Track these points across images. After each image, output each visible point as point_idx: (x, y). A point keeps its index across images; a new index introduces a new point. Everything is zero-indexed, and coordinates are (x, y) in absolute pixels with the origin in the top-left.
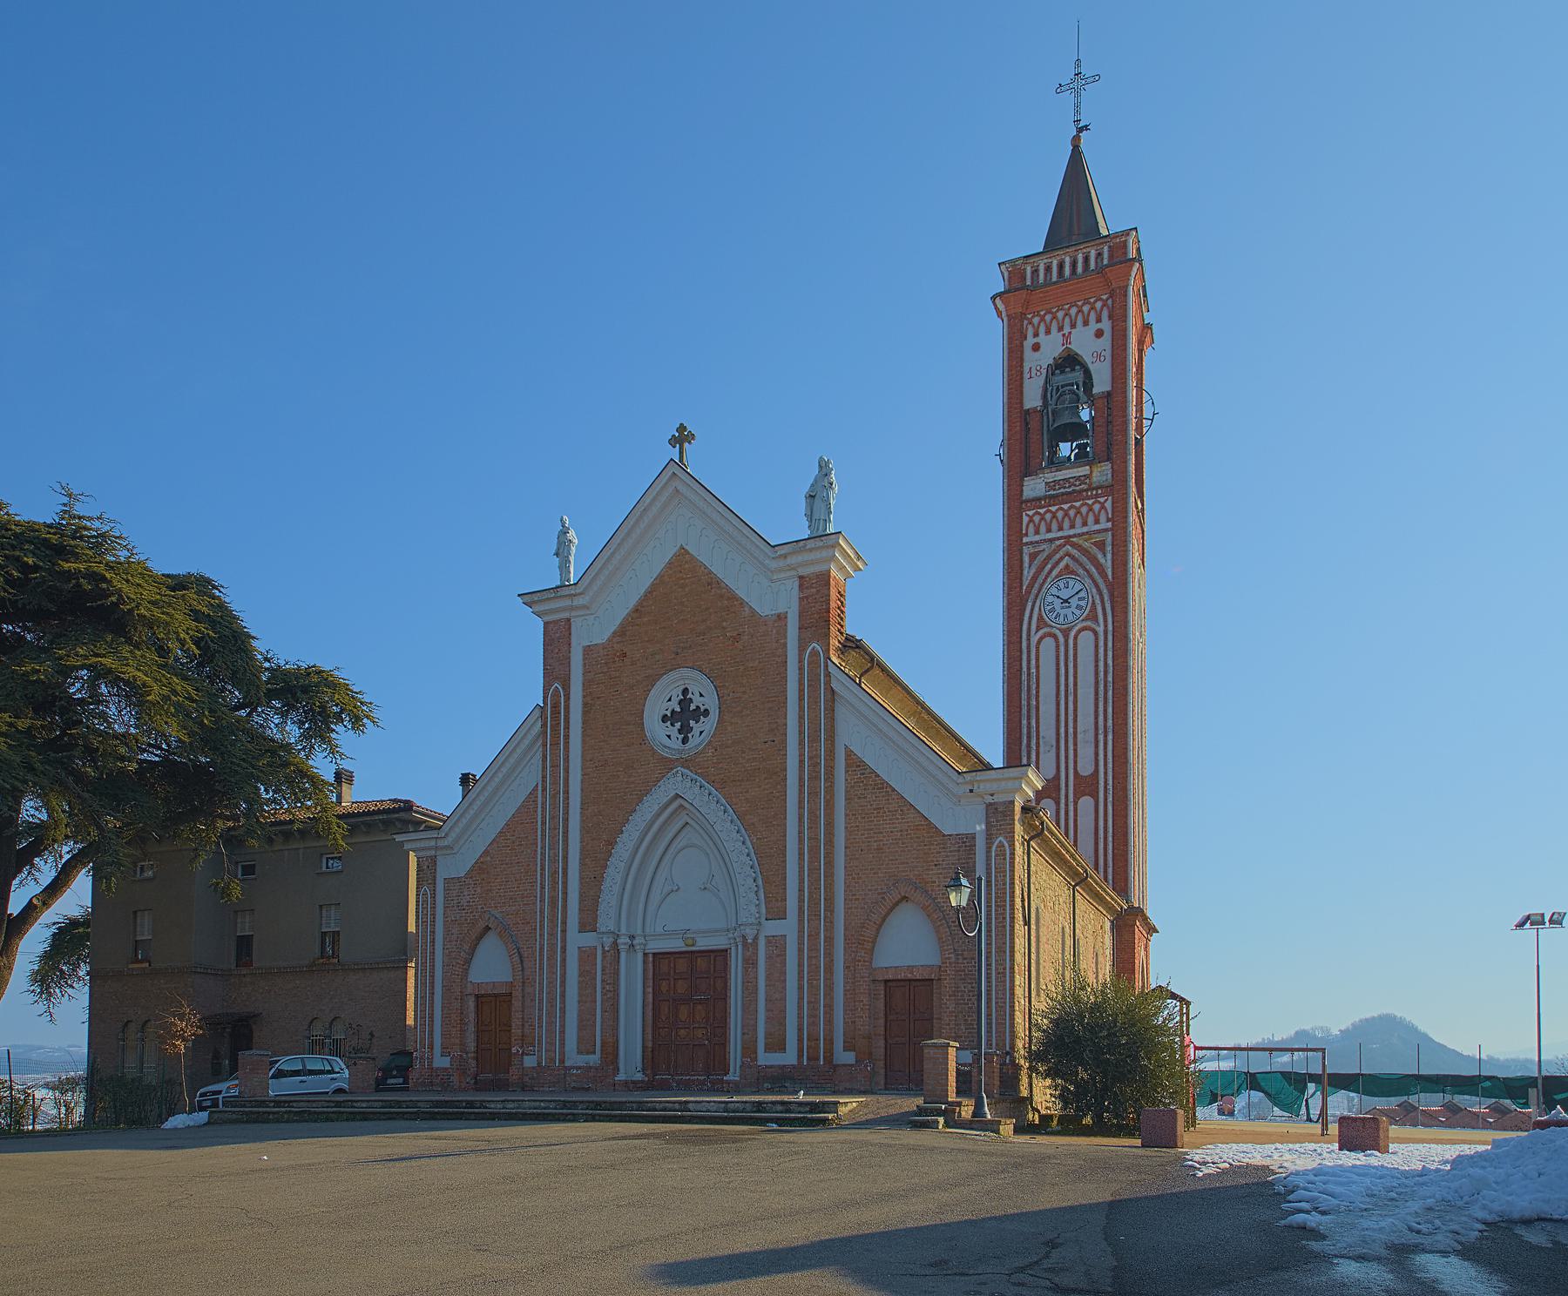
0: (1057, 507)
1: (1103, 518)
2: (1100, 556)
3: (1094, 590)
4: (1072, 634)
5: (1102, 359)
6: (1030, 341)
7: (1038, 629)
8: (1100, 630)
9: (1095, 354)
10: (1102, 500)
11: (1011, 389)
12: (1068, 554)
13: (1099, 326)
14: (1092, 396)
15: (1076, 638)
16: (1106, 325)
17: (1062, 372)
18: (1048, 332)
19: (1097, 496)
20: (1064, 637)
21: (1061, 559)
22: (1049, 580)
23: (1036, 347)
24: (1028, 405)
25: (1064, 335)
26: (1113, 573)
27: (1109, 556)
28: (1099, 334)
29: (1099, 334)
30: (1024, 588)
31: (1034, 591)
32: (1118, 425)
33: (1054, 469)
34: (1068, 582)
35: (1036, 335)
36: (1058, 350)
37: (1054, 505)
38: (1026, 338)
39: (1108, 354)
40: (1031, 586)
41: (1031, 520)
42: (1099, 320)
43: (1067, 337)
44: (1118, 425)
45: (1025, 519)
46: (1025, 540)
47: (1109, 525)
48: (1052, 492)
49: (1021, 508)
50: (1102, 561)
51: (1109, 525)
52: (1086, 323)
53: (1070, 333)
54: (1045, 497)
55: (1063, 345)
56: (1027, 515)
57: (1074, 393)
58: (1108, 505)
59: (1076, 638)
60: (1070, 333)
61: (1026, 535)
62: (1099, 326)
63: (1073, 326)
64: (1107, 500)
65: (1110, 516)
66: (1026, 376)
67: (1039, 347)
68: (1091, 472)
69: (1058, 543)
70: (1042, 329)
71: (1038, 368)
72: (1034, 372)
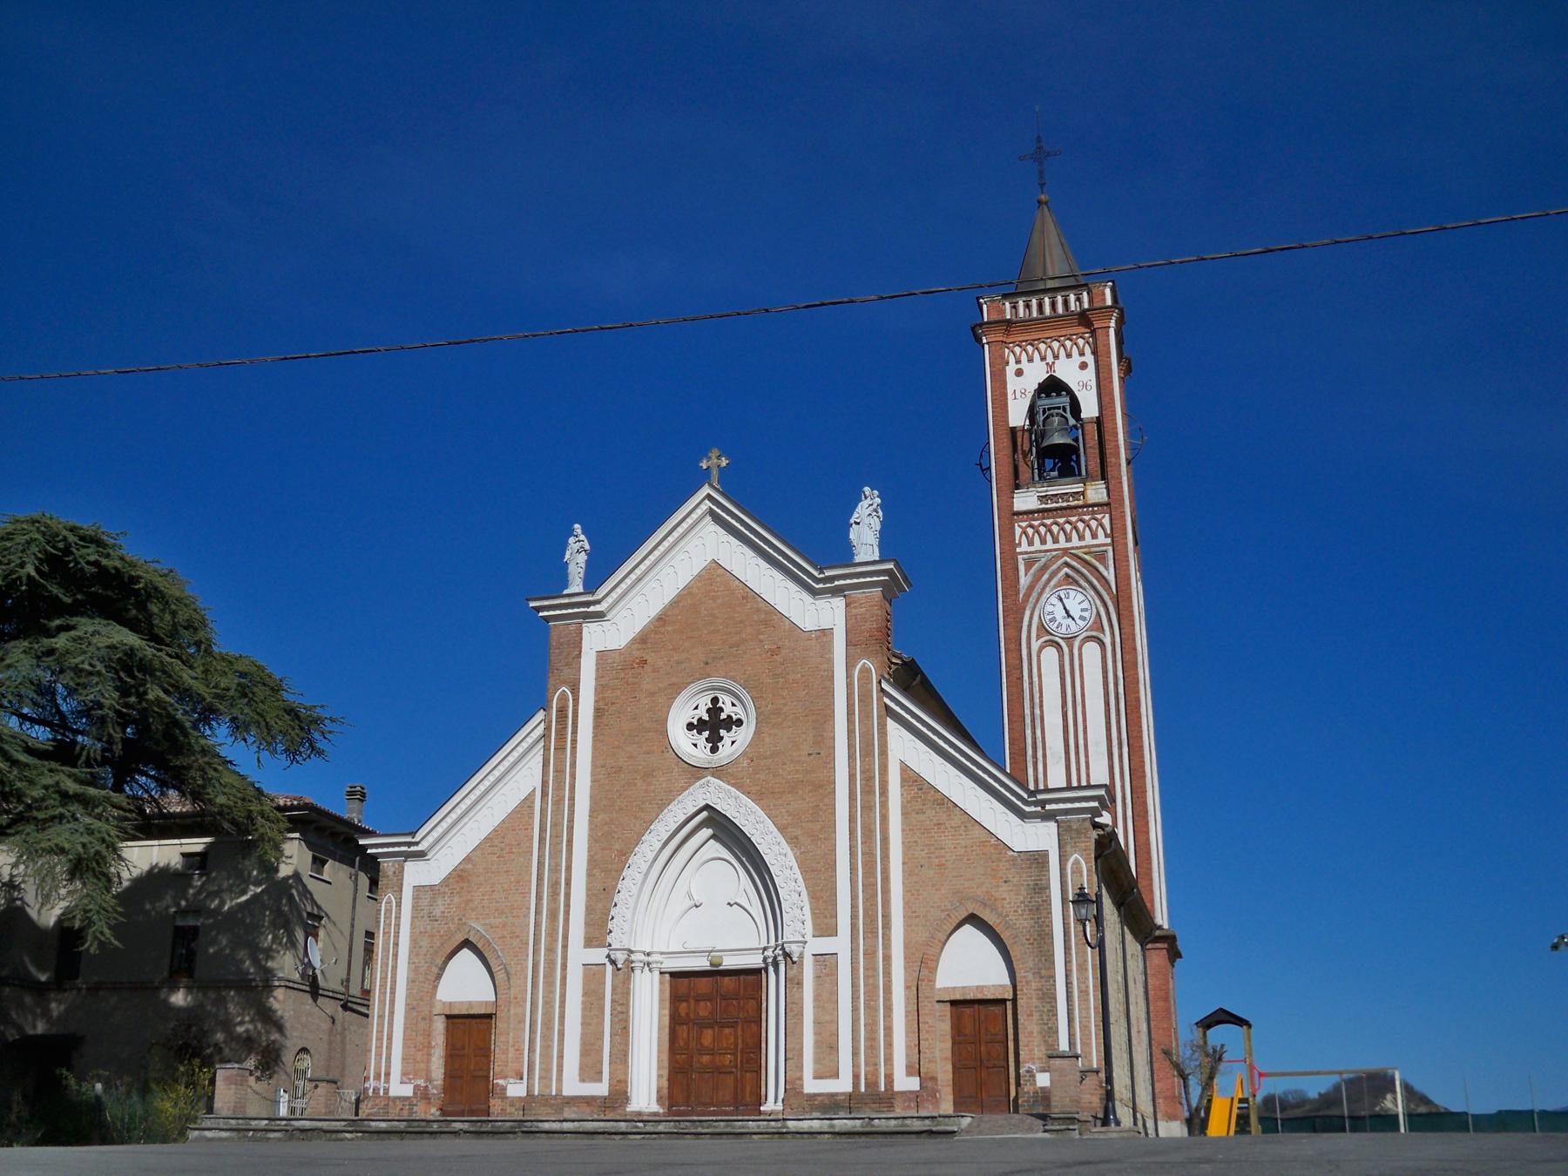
1: (1100, 532)
2: (1101, 568)
3: (1098, 602)
4: (1077, 644)
5: (1089, 388)
6: (1011, 369)
7: (1038, 637)
8: (1107, 640)
9: (1081, 384)
10: (1099, 516)
11: (996, 408)
12: (1067, 564)
13: (1083, 359)
14: (1082, 420)
15: (1080, 649)
16: (1089, 358)
17: (1048, 396)
18: (1030, 360)
19: (1093, 513)
20: (1068, 646)
21: (1059, 569)
22: (1048, 589)
23: (1019, 373)
25: (1047, 364)
28: (1083, 366)
29: (1083, 366)
30: (1021, 596)
31: (1032, 600)
34: (1068, 593)
35: (1018, 362)
37: (1049, 518)
38: (1008, 363)
40: (1028, 595)
42: (1082, 354)
43: (1050, 366)
45: (1018, 531)
46: (1018, 550)
47: (1109, 540)
48: (1044, 506)
50: (1105, 573)
52: (1069, 356)
53: (1053, 363)
54: (1038, 511)
55: (1048, 372)
56: (1019, 526)
57: (1062, 416)
58: (1106, 521)
59: (1080, 649)
60: (1053, 363)
61: (1020, 544)
62: (1083, 359)
63: (1056, 357)
64: (1103, 517)
65: (1109, 532)
68: (1085, 490)
69: (1054, 553)
70: (1024, 357)
71: (1023, 391)
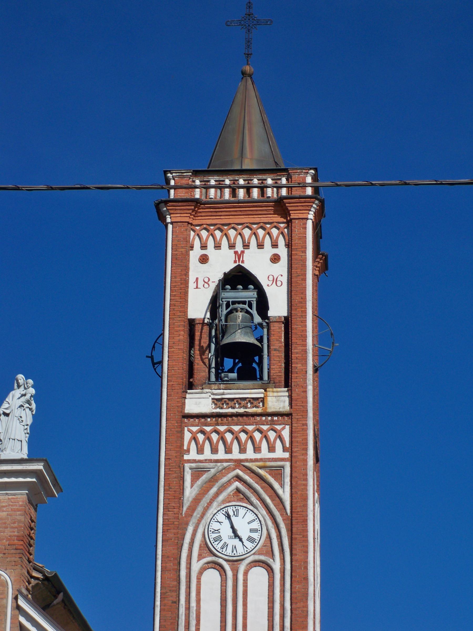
0: (225, 427)
1: (278, 444)
2: (276, 485)
3: (270, 523)
5: (279, 283)
6: (195, 254)
9: (271, 278)
10: (278, 427)
11: (175, 296)
12: (238, 478)
13: (275, 251)
14: (268, 318)
17: (234, 288)
18: (218, 246)
21: (229, 483)
23: (204, 259)
24: (192, 314)
25: (236, 253)
26: (292, 509)
27: (287, 488)
28: (275, 259)
32: (297, 353)
33: (222, 386)
35: (204, 247)
36: (229, 266)
38: (192, 247)
39: (285, 279)
41: (195, 438)
43: (239, 256)
44: (297, 353)
45: (187, 436)
47: (287, 455)
49: (182, 422)
50: (280, 491)
51: (287, 455)
52: (260, 246)
53: (243, 252)
56: (189, 431)
57: (247, 312)
58: (286, 434)
60: (243, 252)
62: (275, 251)
63: (246, 246)
65: (288, 445)
66: (192, 285)
67: (208, 259)
69: (225, 464)
70: (211, 243)
71: (206, 280)
72: (201, 283)
